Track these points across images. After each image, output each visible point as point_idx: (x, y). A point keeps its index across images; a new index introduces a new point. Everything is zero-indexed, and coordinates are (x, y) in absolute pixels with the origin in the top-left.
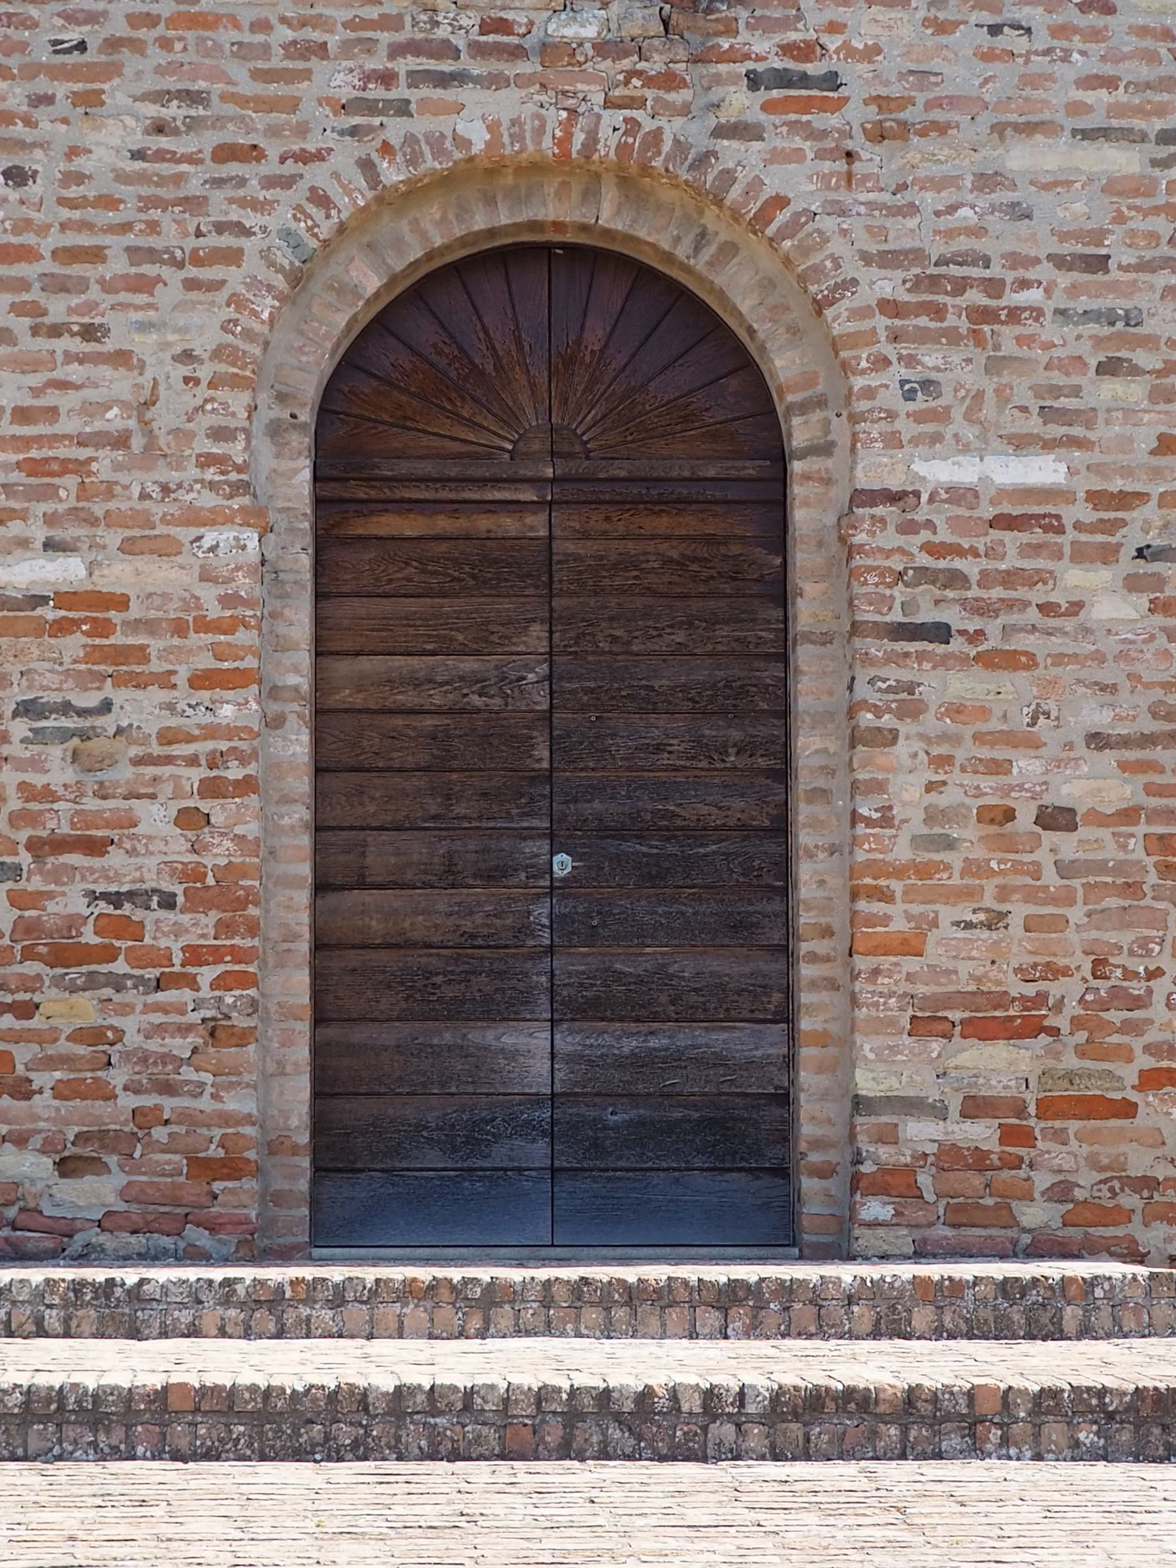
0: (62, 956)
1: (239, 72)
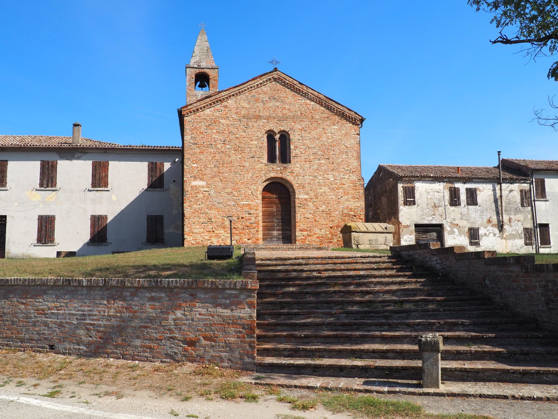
0: (248, 227)
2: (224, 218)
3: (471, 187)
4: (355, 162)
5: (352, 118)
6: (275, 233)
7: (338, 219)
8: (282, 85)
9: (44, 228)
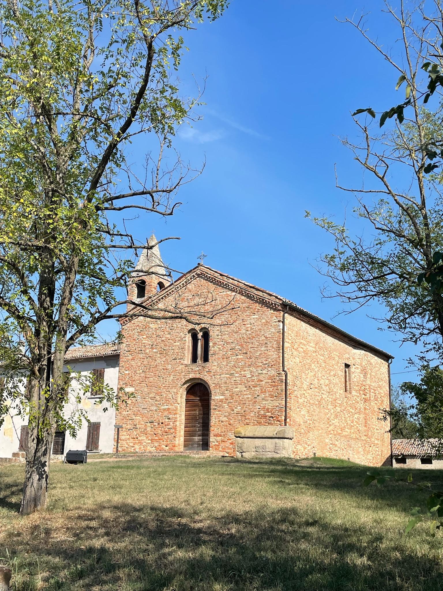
0: (166, 432)
1: (178, 374)
2: (147, 424)
4: (274, 354)
5: (272, 304)
6: (196, 438)
7: (253, 421)
8: (205, 280)
9: (91, 434)
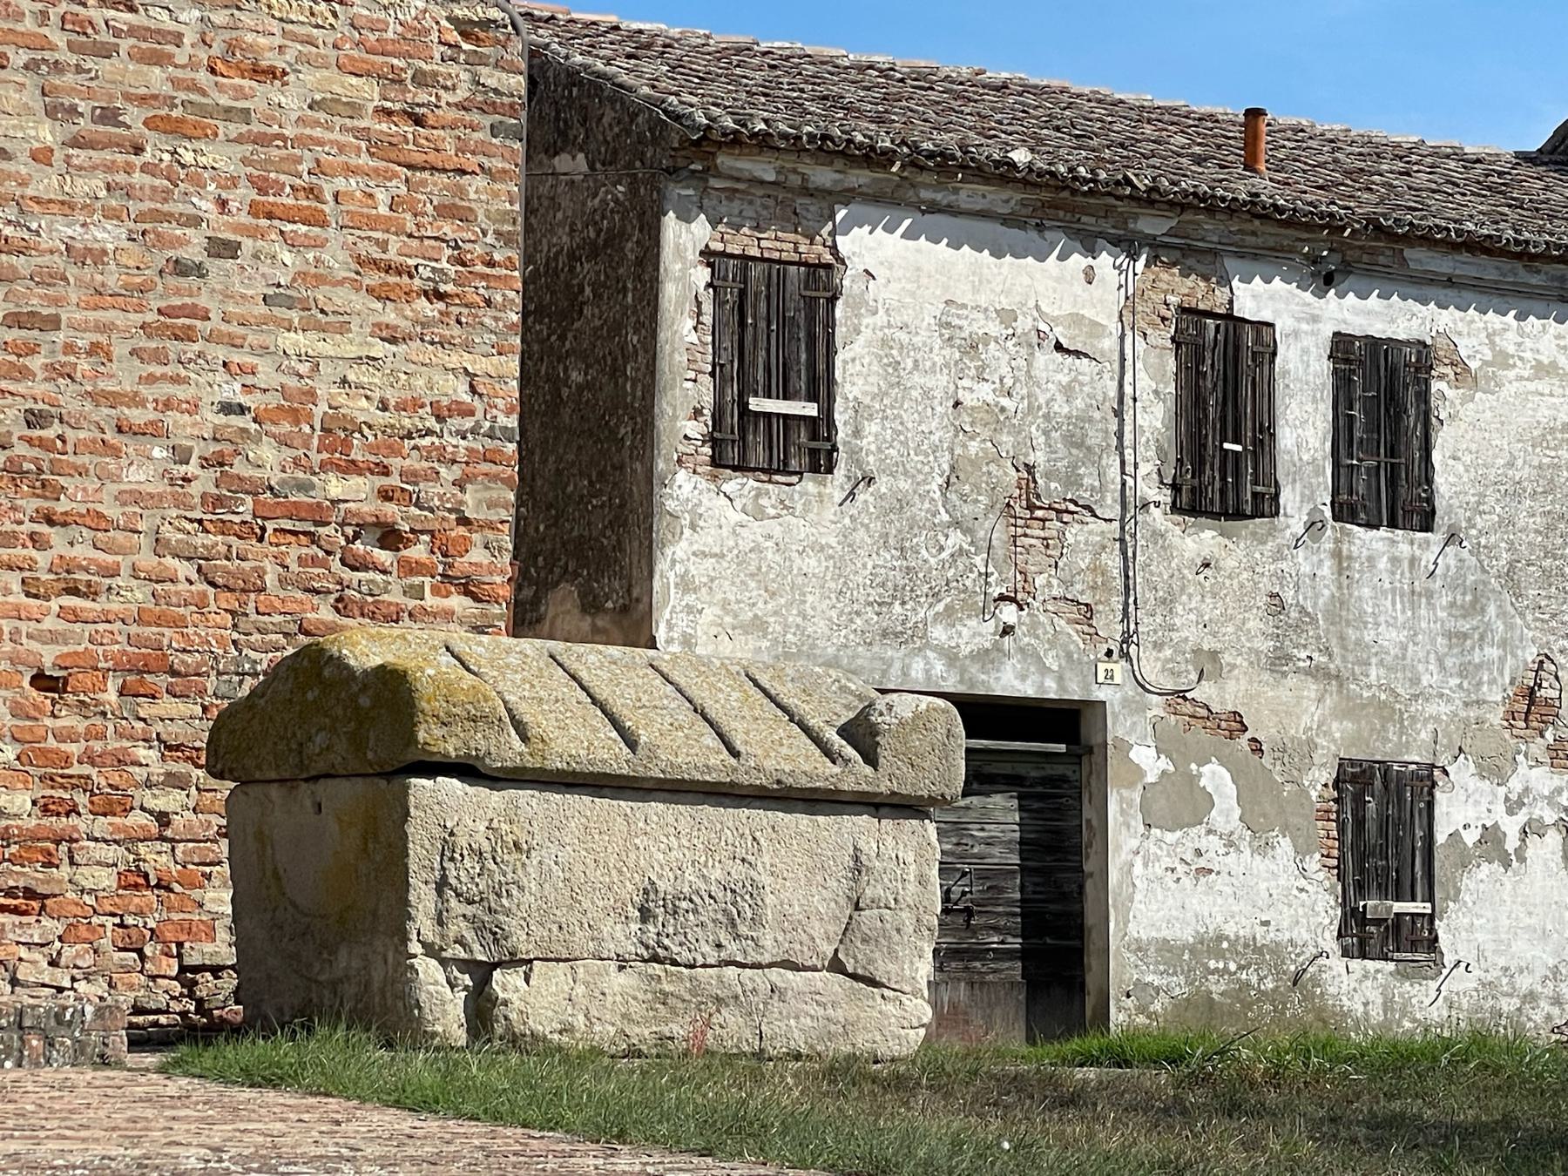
3: (1379, 329)
7: (147, 560)
